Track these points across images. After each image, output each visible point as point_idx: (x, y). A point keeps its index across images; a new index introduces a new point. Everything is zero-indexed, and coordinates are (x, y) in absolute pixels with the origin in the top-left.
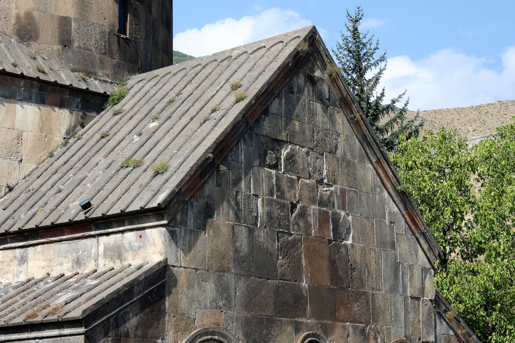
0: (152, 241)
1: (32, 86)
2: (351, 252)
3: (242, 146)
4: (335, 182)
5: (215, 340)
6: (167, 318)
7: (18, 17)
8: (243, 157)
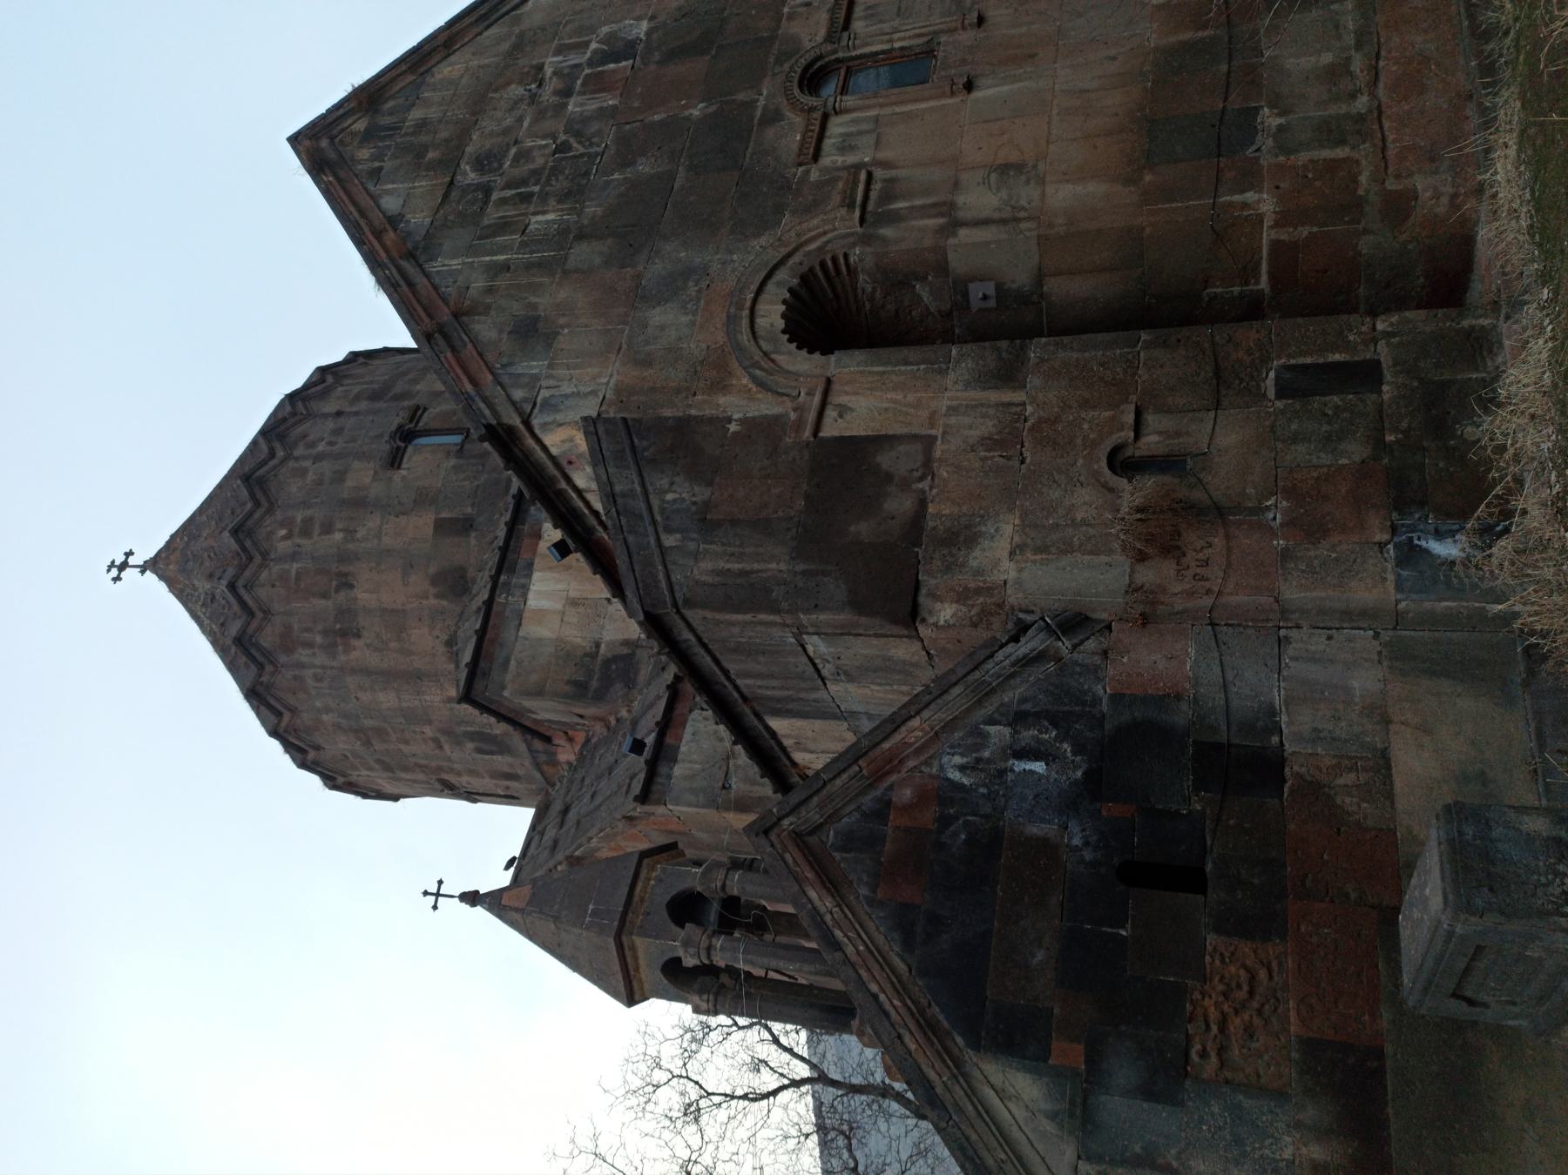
0: (567, 445)
1: (507, 584)
2: (661, 18)
3: (435, 267)
4: (540, 67)
5: (755, 301)
6: (693, 412)
7: (437, 596)
8: (455, 262)
